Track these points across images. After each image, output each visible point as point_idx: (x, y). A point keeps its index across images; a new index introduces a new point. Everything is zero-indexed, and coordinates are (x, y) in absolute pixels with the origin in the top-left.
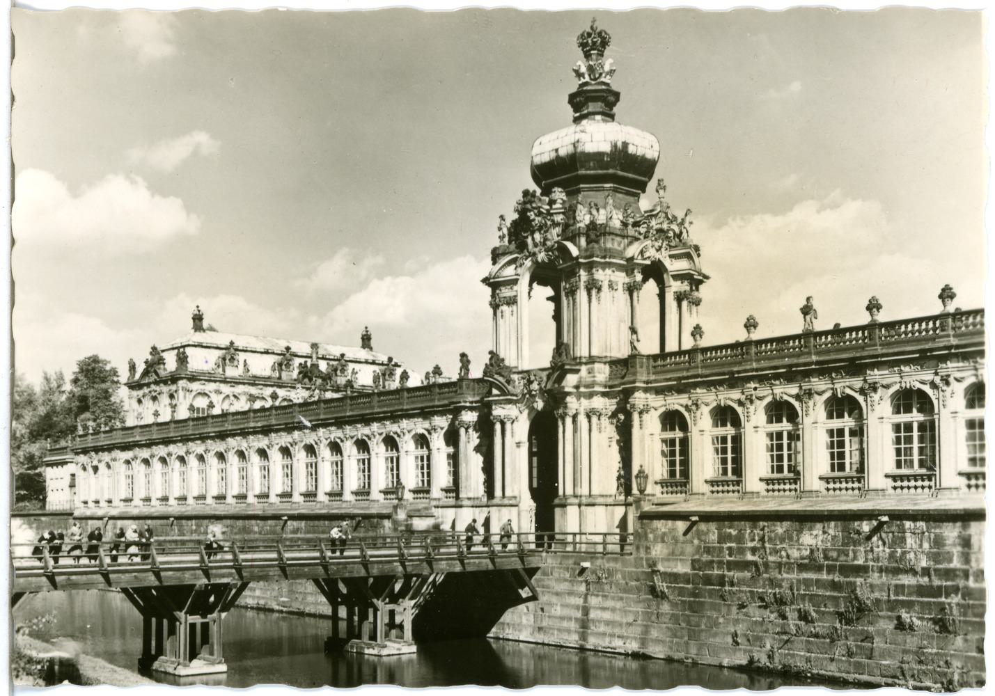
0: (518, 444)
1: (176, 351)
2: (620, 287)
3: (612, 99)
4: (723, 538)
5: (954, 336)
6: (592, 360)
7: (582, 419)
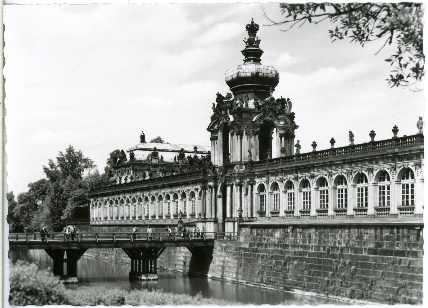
4: (258, 234)
7: (234, 186)
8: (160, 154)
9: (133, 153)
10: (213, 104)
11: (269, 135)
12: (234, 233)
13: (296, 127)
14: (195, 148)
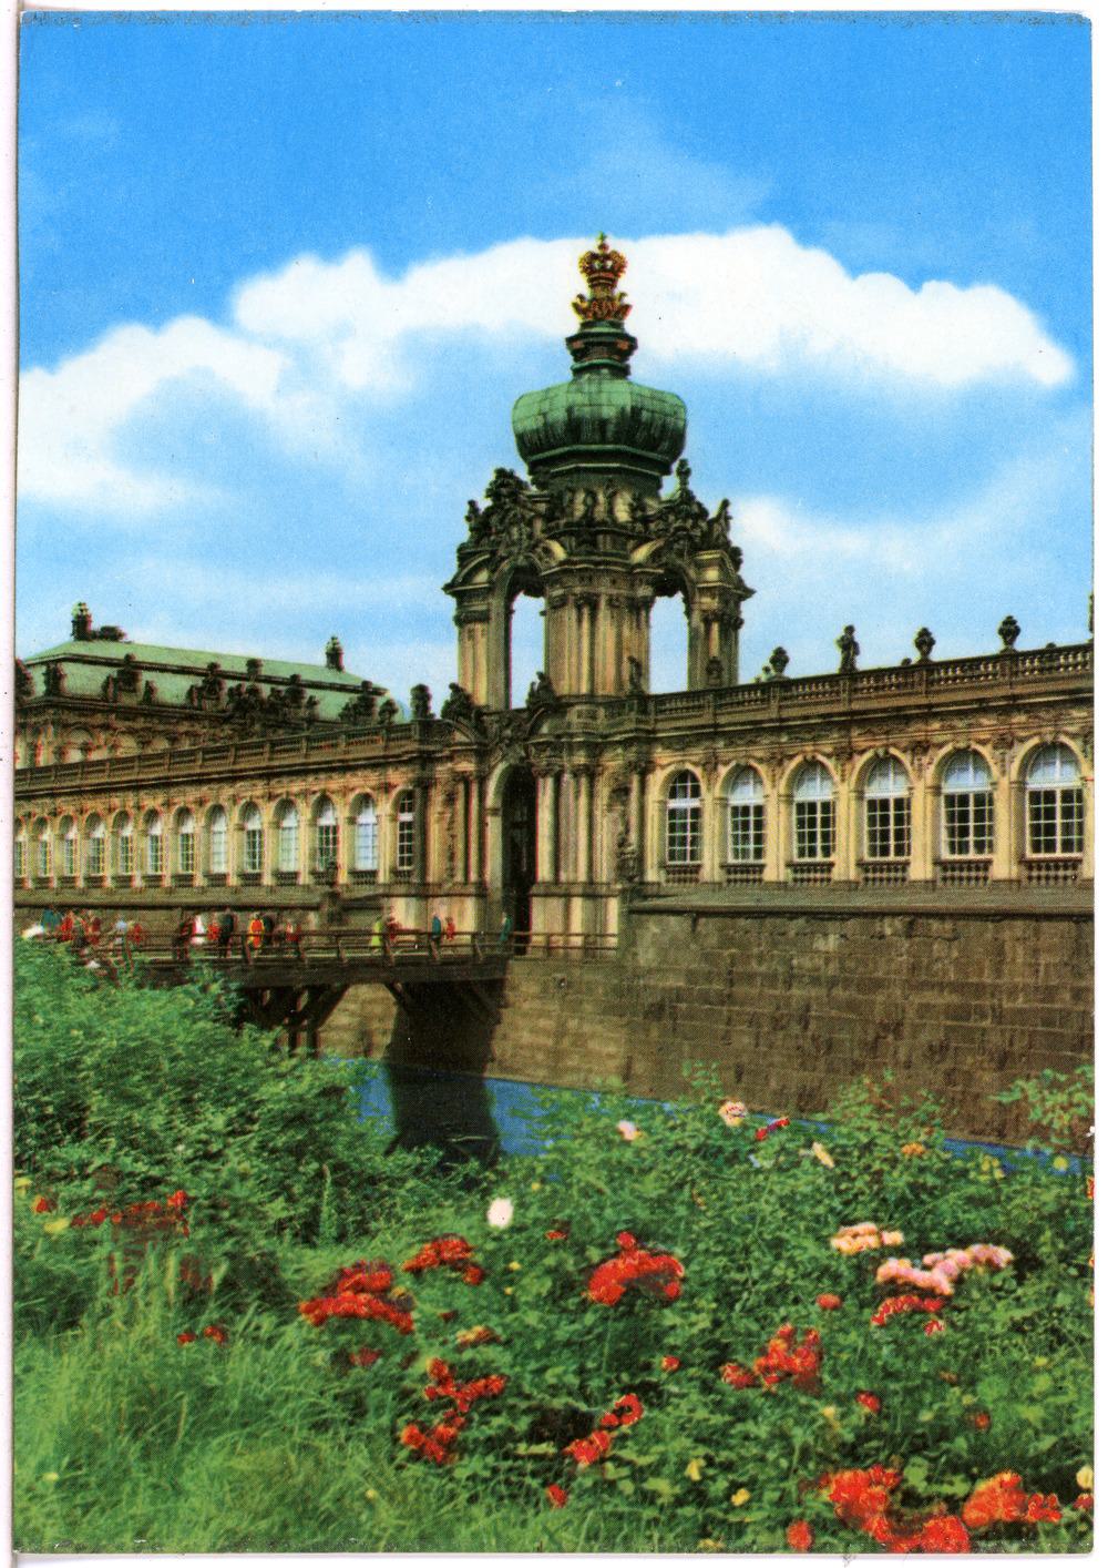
3: (624, 345)
4: (727, 941)
7: (567, 777)
8: (146, 676)
10: (472, 504)
12: (567, 933)
13: (749, 593)
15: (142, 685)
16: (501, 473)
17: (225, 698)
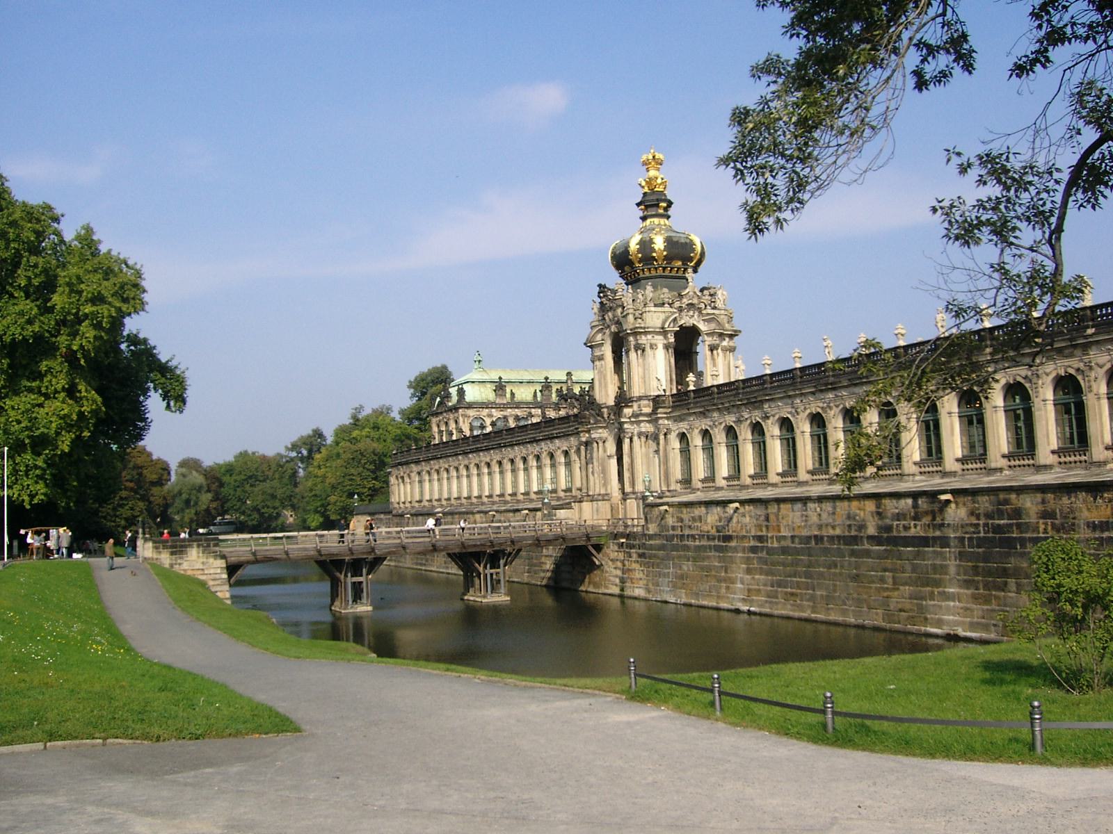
0: (610, 457)
1: (457, 388)
2: (660, 346)
5: (833, 376)
6: (640, 398)
7: (635, 438)
9: (462, 388)
11: (691, 349)
14: (569, 374)
15: (508, 390)
16: (600, 286)
17: (554, 395)
